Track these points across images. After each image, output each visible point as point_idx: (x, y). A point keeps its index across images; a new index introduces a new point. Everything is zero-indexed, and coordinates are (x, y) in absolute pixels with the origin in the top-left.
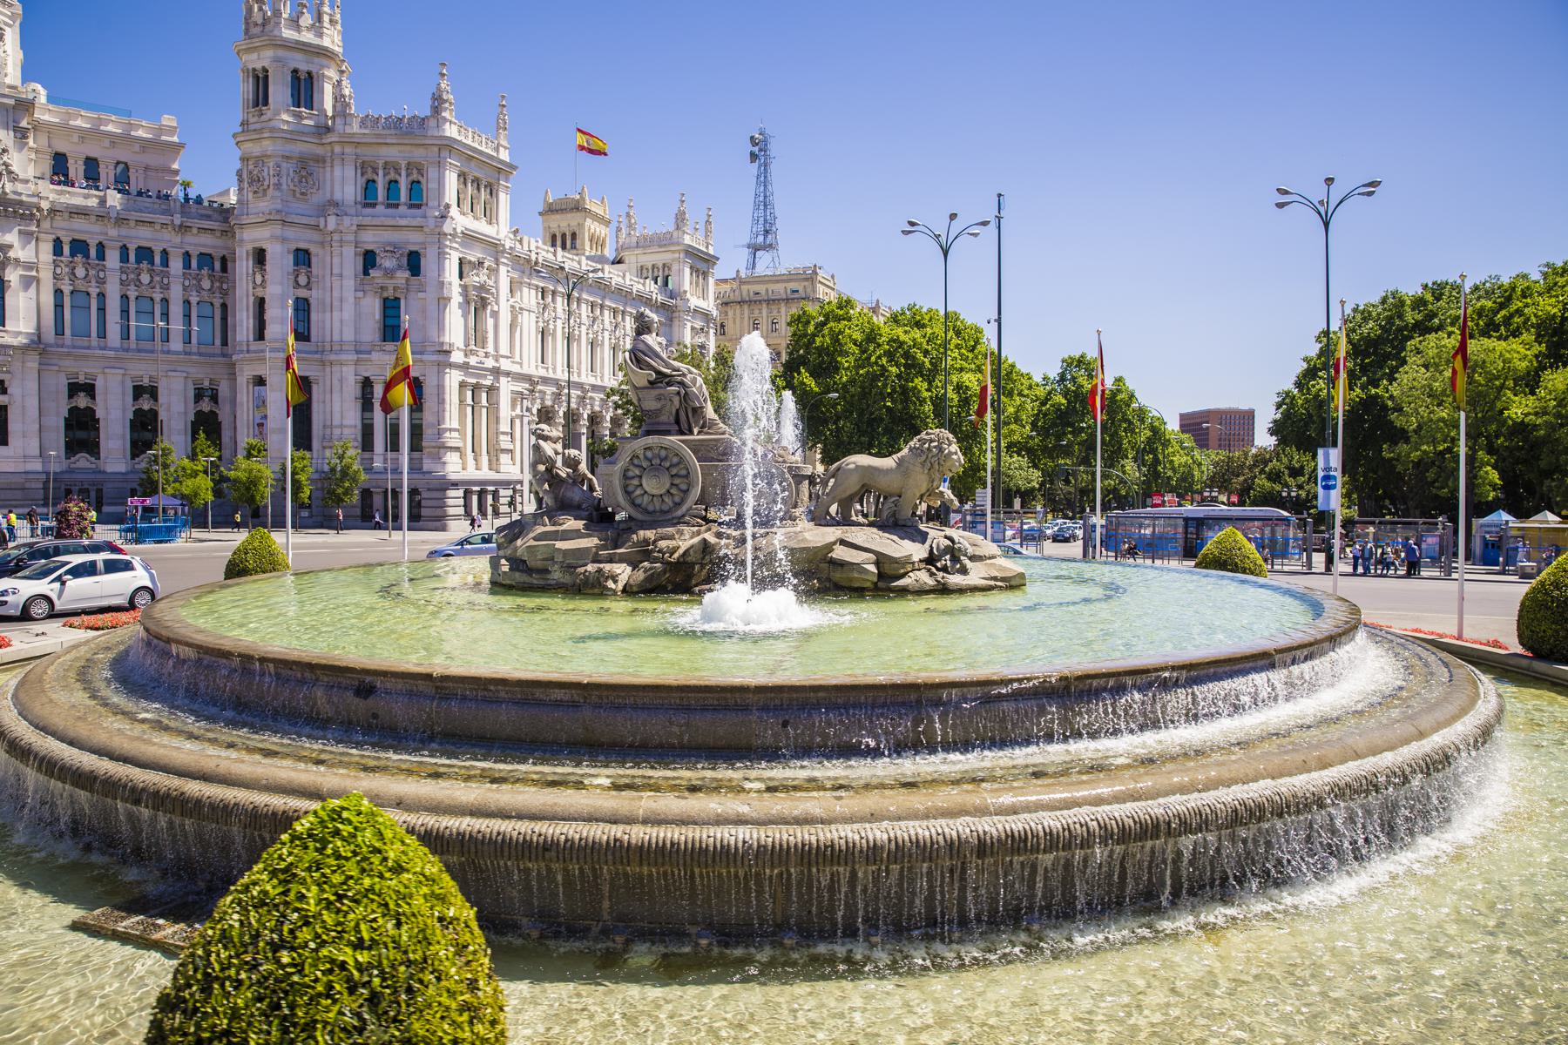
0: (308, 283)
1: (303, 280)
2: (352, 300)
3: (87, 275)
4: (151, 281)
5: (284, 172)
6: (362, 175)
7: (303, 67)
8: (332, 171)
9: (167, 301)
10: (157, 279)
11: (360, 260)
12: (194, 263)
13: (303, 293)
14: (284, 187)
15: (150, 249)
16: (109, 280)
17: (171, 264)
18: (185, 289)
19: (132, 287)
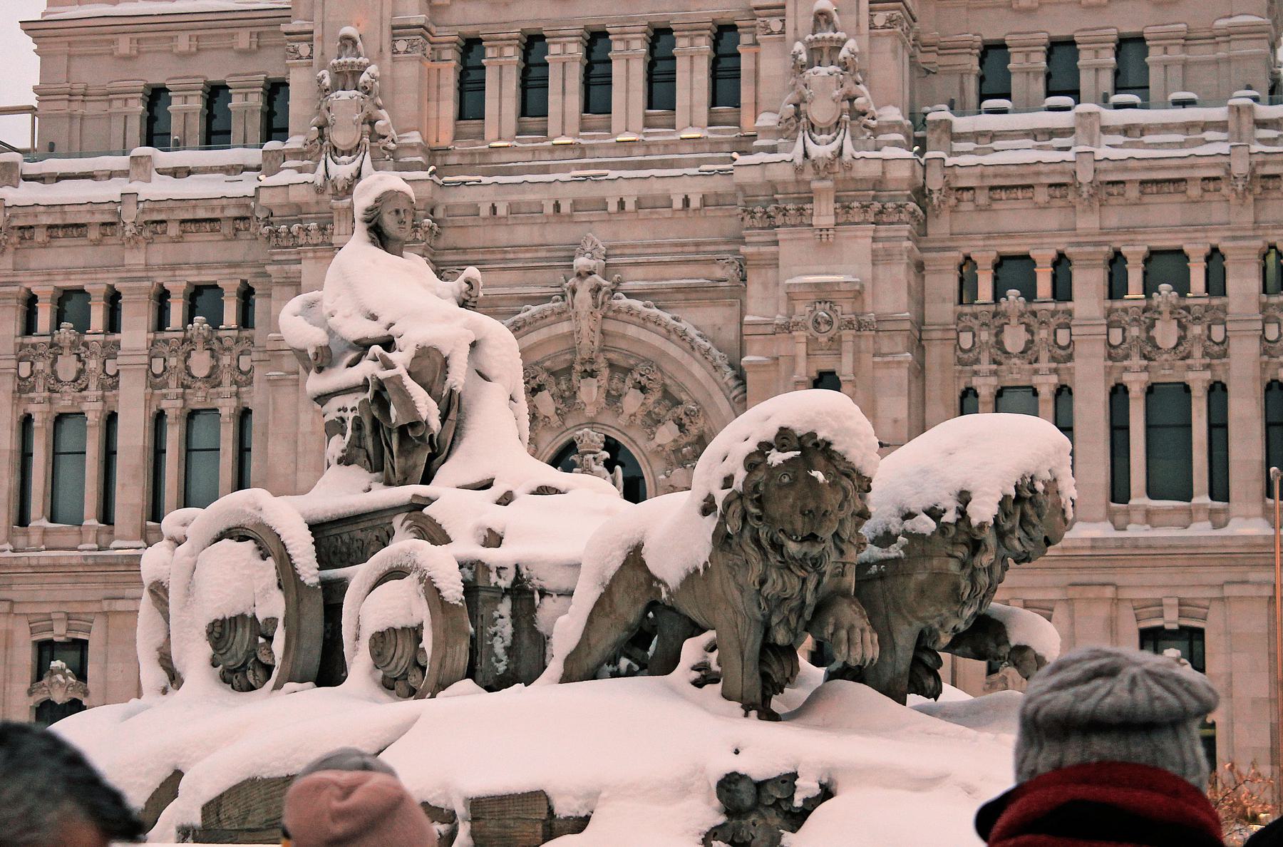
3: (1030, 343)
4: (1181, 340)
9: (1224, 388)
10: (1197, 330)
12: (1135, 278)
15: (1179, 252)
16: (1079, 349)
17: (1231, 284)
18: (1265, 352)
19: (1136, 361)
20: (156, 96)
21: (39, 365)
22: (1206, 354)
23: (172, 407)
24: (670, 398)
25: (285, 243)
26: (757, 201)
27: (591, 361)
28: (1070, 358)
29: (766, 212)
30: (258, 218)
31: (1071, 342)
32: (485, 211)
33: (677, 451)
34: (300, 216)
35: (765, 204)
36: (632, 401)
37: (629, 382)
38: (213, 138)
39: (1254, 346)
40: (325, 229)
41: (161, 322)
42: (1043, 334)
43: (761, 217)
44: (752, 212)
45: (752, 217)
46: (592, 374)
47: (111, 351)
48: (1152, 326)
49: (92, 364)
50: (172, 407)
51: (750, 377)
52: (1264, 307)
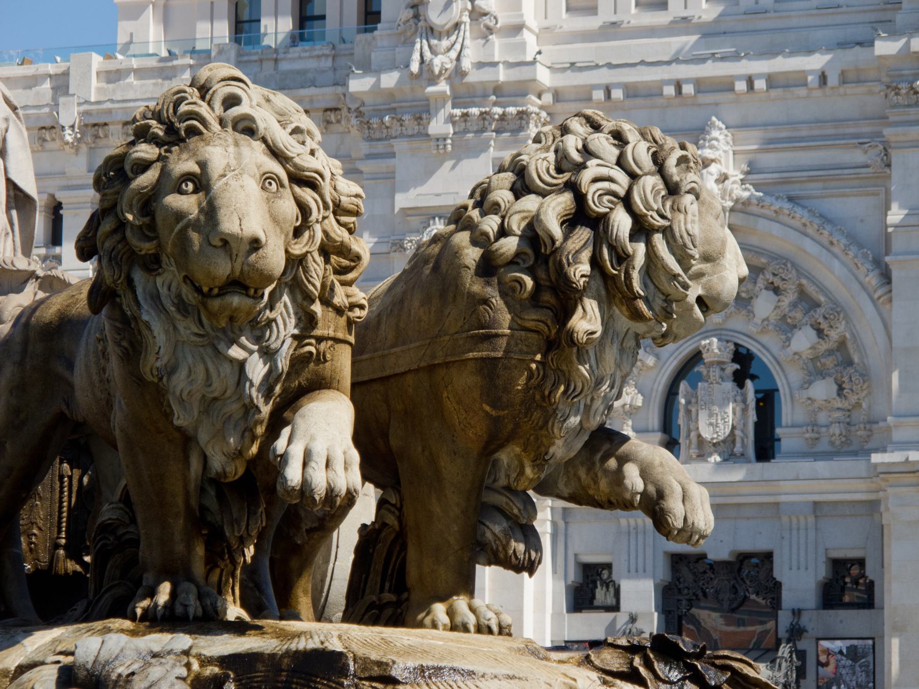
24: (807, 303)
25: (378, 135)
26: (902, 75)
29: (912, 88)
30: (349, 109)
33: (815, 359)
34: (394, 105)
35: (910, 78)
37: (761, 283)
38: (308, 23)
40: (421, 118)
43: (907, 93)
44: (896, 88)
45: (897, 94)
51: (895, 275)
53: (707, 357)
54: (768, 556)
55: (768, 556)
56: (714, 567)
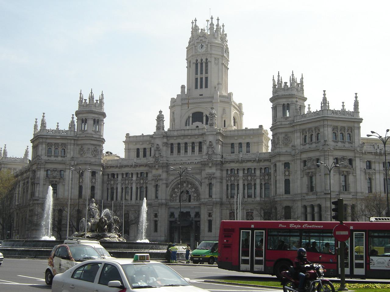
0: (289, 174)
1: (287, 173)
2: (300, 178)
3: (234, 179)
5: (280, 139)
6: (303, 135)
7: (286, 103)
8: (294, 135)
11: (302, 164)
13: (287, 178)
14: (281, 143)
18: (260, 180)
19: (246, 181)
20: (138, 149)
21: (124, 182)
22: (254, 180)
23: (139, 186)
27: (185, 181)
28: (239, 181)
31: (239, 179)
32: (173, 164)
36: (190, 186)
39: (259, 179)
41: (138, 177)
42: (236, 178)
46: (185, 183)
47: (132, 180)
48: (248, 177)
49: (130, 181)
50: (139, 186)
52: (260, 175)
53: (184, 192)
54: (190, 212)
55: (190, 212)
56: (184, 213)
